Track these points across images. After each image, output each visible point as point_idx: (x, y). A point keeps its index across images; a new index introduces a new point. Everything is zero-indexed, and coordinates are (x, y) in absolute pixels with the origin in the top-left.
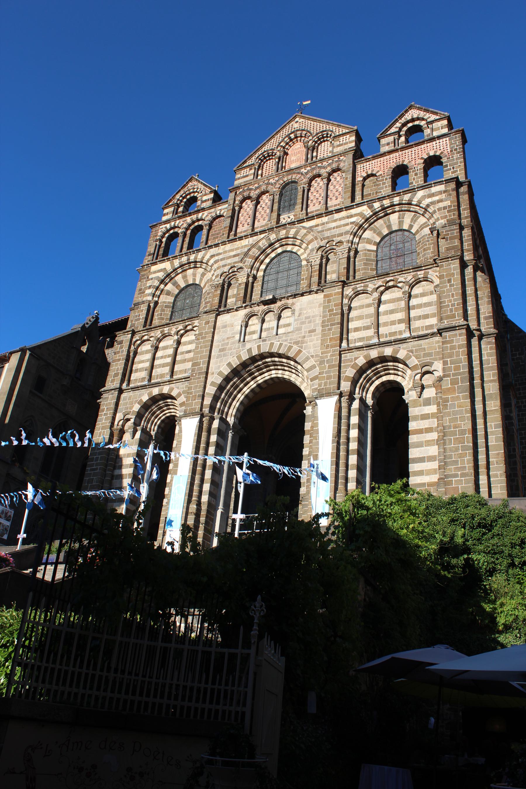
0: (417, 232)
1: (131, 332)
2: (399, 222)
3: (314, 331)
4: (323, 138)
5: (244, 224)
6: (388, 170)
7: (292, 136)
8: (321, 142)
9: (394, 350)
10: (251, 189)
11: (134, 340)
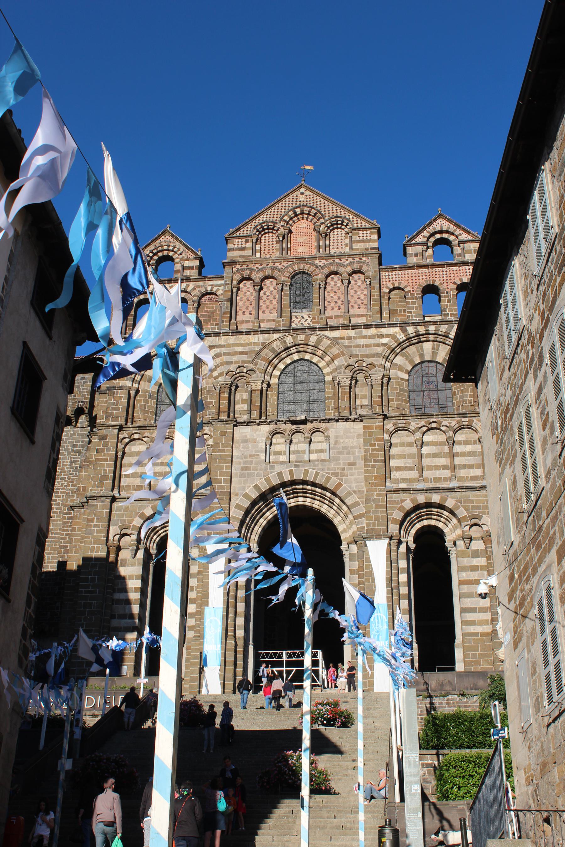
1: (118, 427)
2: (433, 353)
3: (353, 464)
4: (337, 224)
6: (418, 288)
7: (298, 211)
8: (334, 229)
9: (441, 498)
10: (251, 270)
11: (121, 436)
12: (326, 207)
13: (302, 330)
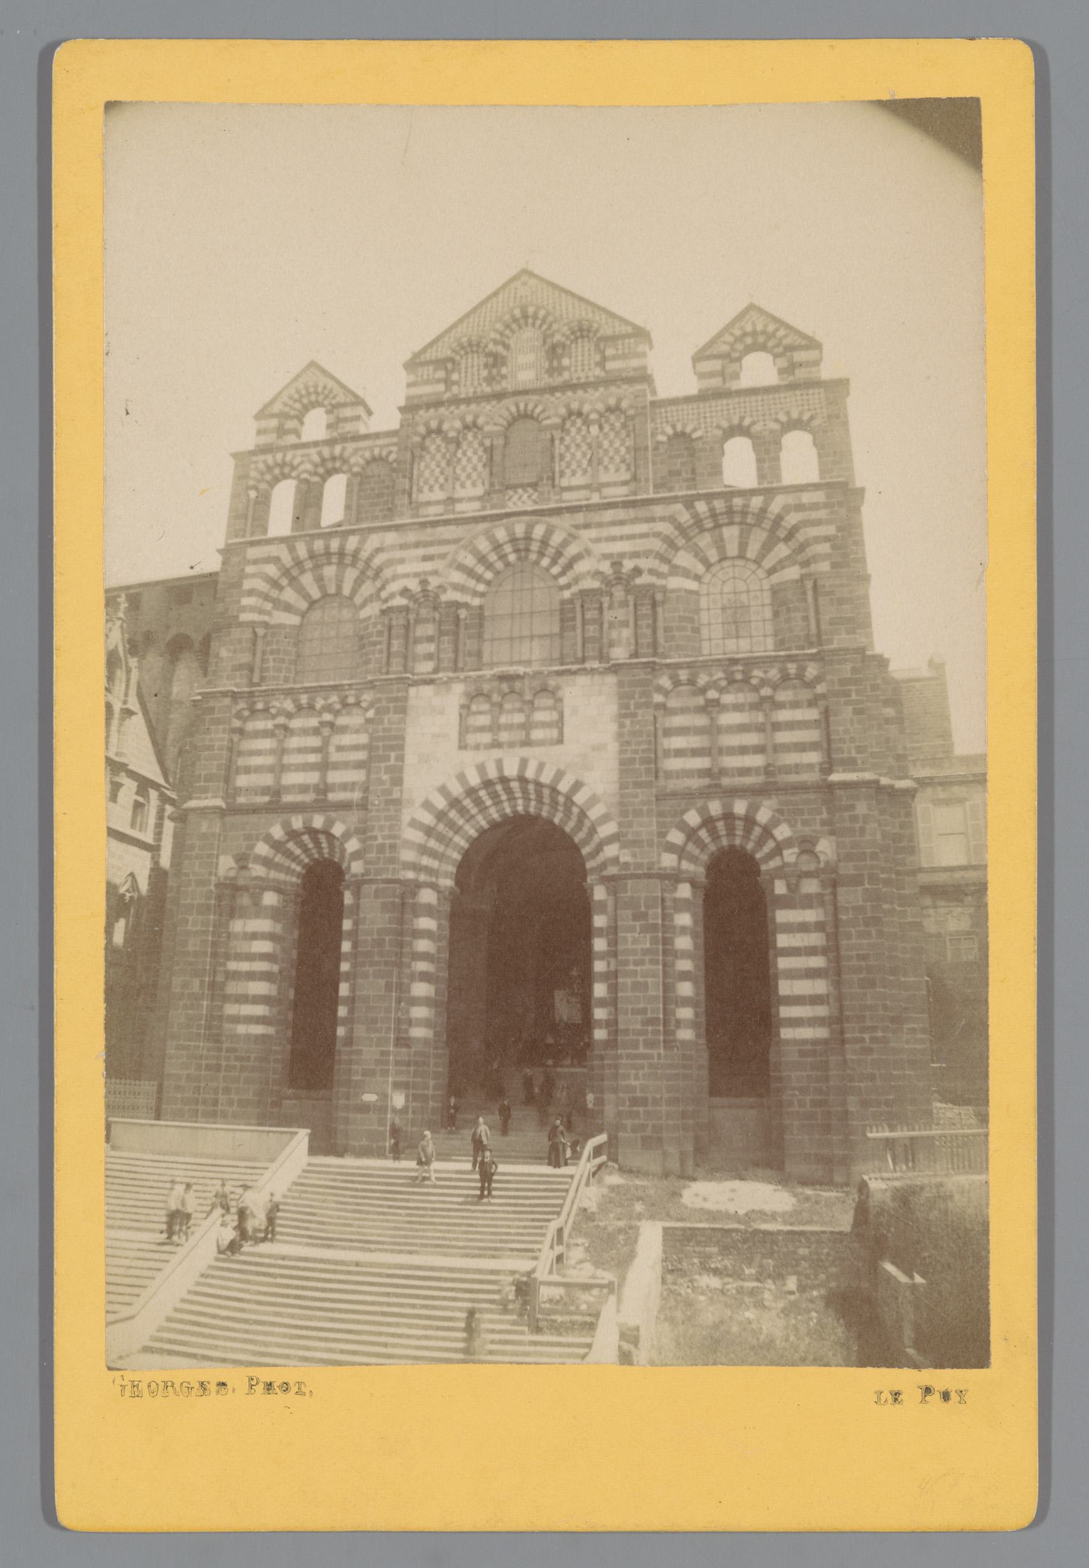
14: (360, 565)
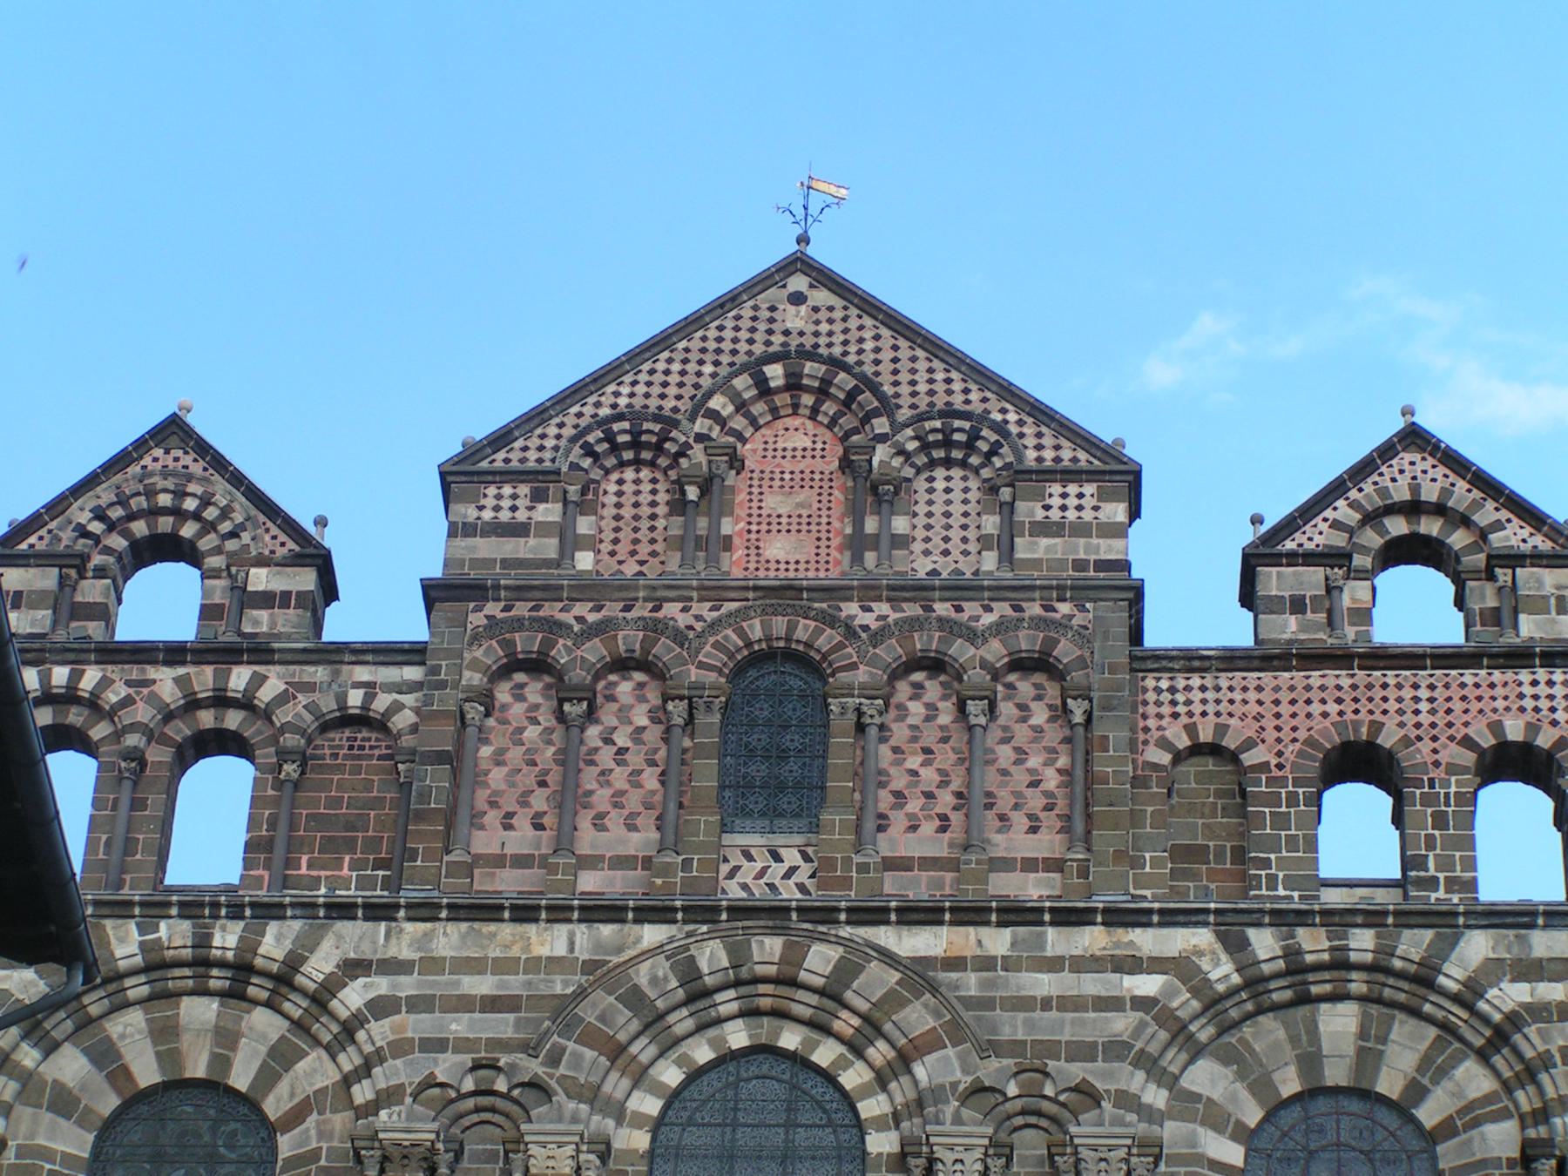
0: (1447, 1129)
2: (1361, 1052)
5: (509, 815)
6: (1300, 754)
7: (775, 373)
10: (554, 628)
12: (904, 365)
13: (773, 914)
14: (295, 1007)
